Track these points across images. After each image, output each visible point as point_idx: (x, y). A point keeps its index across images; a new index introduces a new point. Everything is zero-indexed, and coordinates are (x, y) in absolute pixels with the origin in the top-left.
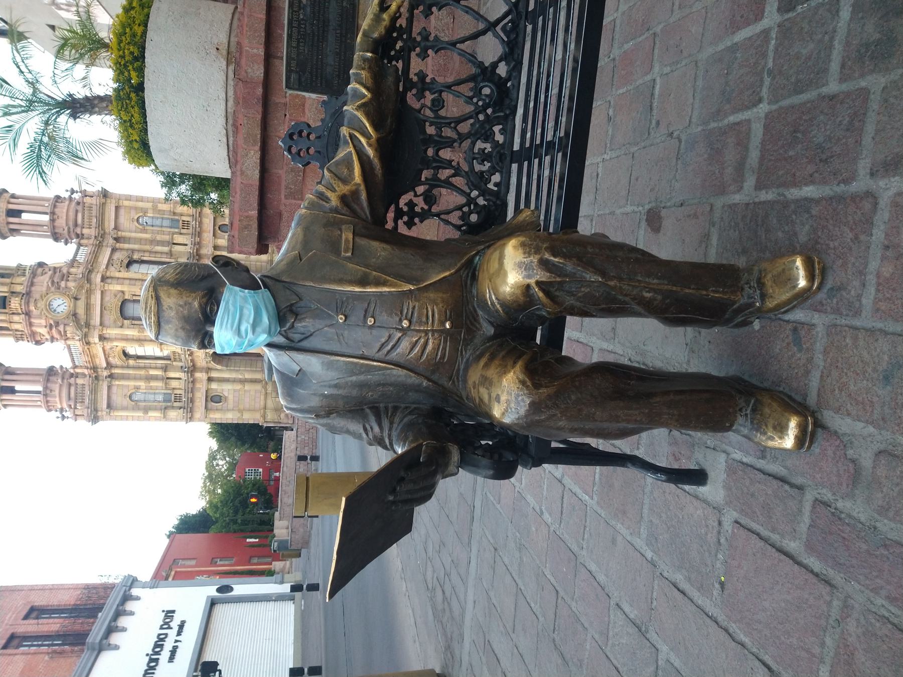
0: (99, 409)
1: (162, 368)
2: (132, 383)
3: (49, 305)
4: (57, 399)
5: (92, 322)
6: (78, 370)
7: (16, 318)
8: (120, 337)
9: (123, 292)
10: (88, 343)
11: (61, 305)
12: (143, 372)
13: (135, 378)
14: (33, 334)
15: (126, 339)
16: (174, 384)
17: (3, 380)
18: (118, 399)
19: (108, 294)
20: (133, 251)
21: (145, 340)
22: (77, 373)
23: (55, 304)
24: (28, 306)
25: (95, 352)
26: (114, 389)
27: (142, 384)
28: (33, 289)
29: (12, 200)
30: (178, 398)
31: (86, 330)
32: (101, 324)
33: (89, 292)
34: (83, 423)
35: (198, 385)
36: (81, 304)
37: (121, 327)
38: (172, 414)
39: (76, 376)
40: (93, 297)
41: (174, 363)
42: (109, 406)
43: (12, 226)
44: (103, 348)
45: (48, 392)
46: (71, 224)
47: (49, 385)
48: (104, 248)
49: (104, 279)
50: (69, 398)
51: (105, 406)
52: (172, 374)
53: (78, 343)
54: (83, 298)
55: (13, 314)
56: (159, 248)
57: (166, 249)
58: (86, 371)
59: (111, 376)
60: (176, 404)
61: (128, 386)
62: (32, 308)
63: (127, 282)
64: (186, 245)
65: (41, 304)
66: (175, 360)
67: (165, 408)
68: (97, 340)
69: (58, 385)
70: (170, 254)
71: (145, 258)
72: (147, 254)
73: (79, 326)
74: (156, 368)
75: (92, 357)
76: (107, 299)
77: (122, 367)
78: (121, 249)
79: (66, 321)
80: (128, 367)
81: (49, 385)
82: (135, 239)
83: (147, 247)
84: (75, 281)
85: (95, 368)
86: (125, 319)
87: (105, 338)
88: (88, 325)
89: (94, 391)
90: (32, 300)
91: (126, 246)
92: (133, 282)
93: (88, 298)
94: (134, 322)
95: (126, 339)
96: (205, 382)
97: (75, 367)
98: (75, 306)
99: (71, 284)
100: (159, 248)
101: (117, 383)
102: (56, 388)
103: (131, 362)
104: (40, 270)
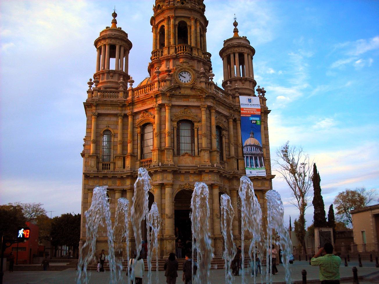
0: (98, 108)
1: (133, 153)
2: (119, 131)
3: (185, 71)
4: (105, 80)
5: (174, 99)
6: (130, 93)
7: (172, 51)
8: (163, 119)
9: (200, 121)
10: (157, 96)
11: (186, 79)
12: (129, 138)
13: (124, 134)
14: (160, 62)
15: (161, 123)
16: (119, 163)
17: (120, 47)
18: (105, 122)
19: (198, 111)
20: (228, 131)
21: (160, 138)
22: (127, 93)
23: (186, 75)
24: (183, 58)
25: (148, 102)
26: (114, 119)
27: (119, 138)
28: (196, 61)
29: (250, 57)
30: (106, 166)
31: (168, 94)
32: (173, 106)
33: (198, 98)
34: (85, 97)
35: (118, 182)
36: (188, 92)
37: (171, 120)
38: (92, 162)
39: (126, 93)
40: (195, 100)
41: (138, 162)
42: (99, 115)
43: (232, 56)
44: (152, 108)
45: (111, 74)
46: (240, 91)
47: (117, 75)
48: (228, 110)
49: (209, 108)
50: (106, 88)
51: (100, 111)
52: (128, 162)
53: (156, 89)
54: (192, 93)
55: (176, 49)
56: (233, 149)
57: (233, 153)
58: (130, 98)
59: (125, 116)
60: (101, 165)
61: (117, 129)
62: (181, 60)
63: (209, 124)
64: (238, 169)
65: (185, 66)
66: (141, 163)
67: (97, 157)
68: (160, 102)
69: (117, 80)
70: (230, 157)
71: (224, 139)
72: (227, 141)
73: (171, 89)
74: (133, 148)
75: (143, 102)
76: (193, 110)
77: (133, 124)
78: (228, 123)
79: (173, 81)
80: (133, 127)
81: (117, 75)
82: (237, 133)
83: (232, 140)
84: (207, 88)
85: (133, 104)
86: (178, 123)
88: (172, 96)
89: (113, 105)
90: (187, 60)
91: (231, 126)
92: (209, 128)
93: (194, 97)
94: (175, 129)
95: (161, 123)
96: (121, 187)
97: (133, 90)
98: (187, 88)
99: (203, 85)
100: (233, 149)
101: (120, 121)
102: (115, 79)
103: (138, 130)
104: (208, 68)
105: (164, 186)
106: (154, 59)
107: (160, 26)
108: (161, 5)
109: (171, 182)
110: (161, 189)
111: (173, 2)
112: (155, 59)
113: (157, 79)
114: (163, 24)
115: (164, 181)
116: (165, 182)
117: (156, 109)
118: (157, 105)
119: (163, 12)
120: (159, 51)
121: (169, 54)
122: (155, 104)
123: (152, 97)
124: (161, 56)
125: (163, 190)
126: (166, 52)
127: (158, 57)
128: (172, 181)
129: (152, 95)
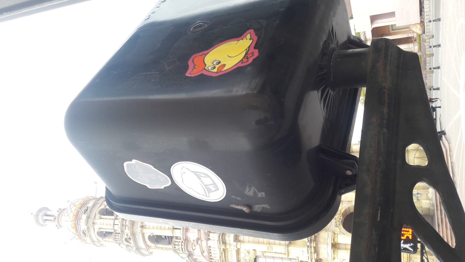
10: (224, 243)
87: (239, 241)
105: (336, 244)
106: (182, 249)
107: (149, 243)
108: (126, 237)
109: (330, 234)
110: (339, 249)
111: (127, 222)
112: (183, 247)
113: (204, 243)
114: (146, 237)
115: (328, 242)
116: (330, 242)
117: (239, 247)
118: (235, 243)
119: (133, 234)
120: (175, 242)
121: (180, 229)
122: (232, 247)
123: (224, 250)
124: (180, 239)
125: (340, 246)
126: (178, 233)
127: (180, 244)
128: (329, 233)
129: (222, 249)
